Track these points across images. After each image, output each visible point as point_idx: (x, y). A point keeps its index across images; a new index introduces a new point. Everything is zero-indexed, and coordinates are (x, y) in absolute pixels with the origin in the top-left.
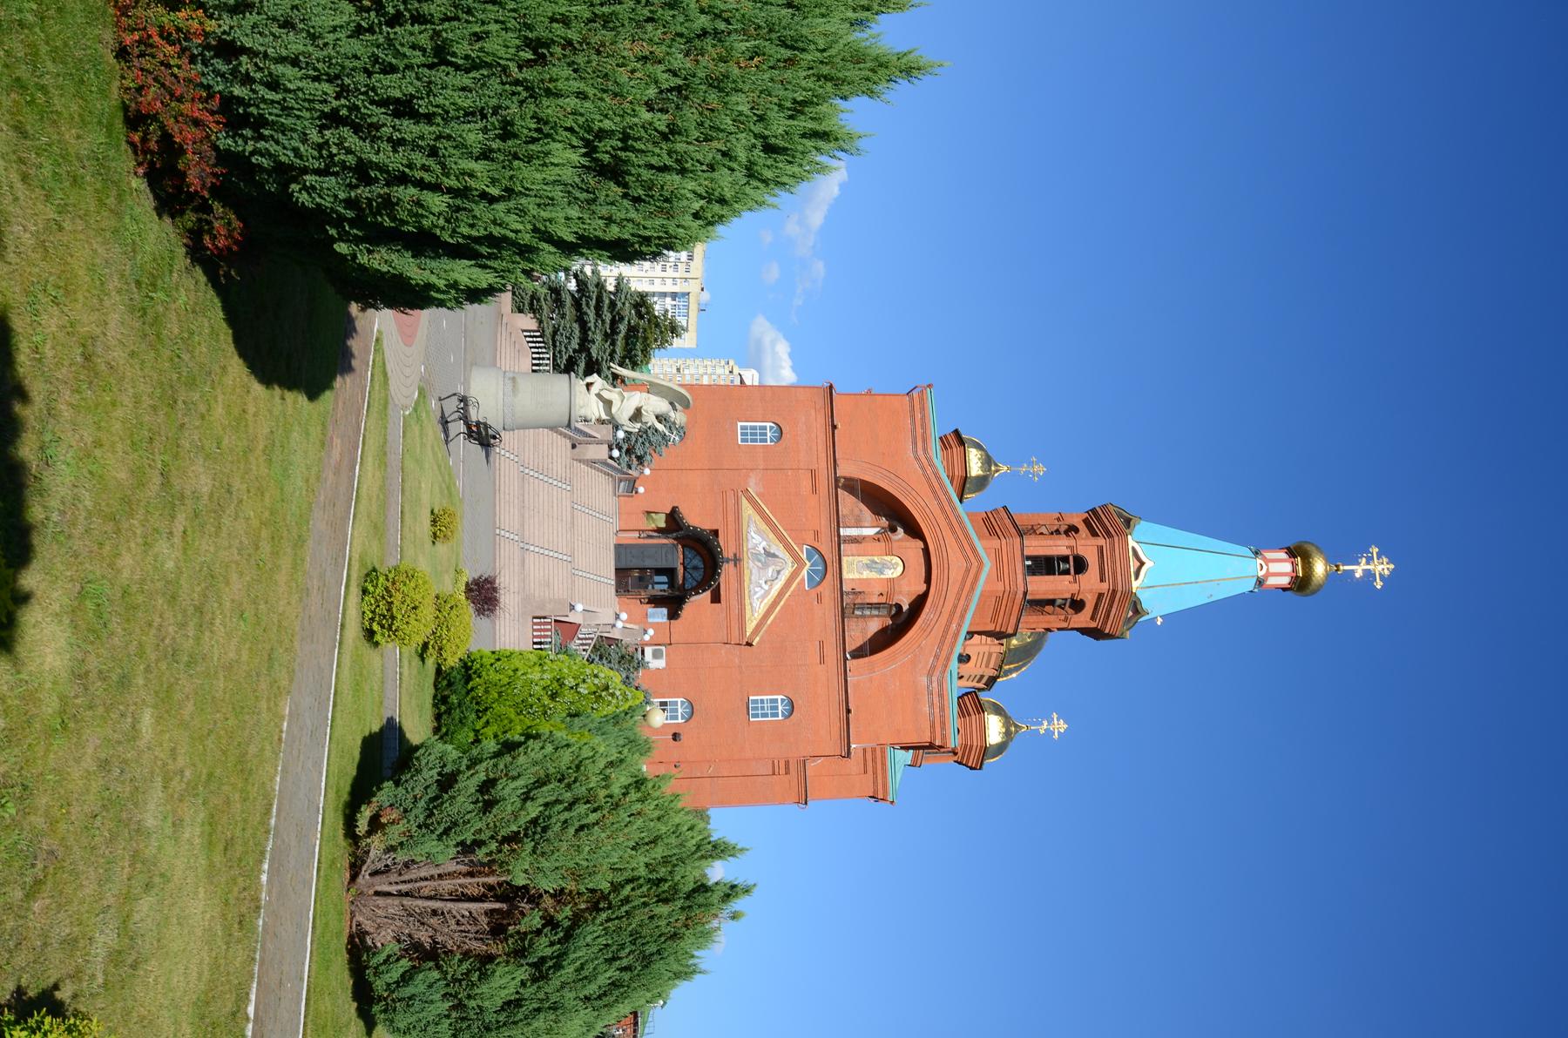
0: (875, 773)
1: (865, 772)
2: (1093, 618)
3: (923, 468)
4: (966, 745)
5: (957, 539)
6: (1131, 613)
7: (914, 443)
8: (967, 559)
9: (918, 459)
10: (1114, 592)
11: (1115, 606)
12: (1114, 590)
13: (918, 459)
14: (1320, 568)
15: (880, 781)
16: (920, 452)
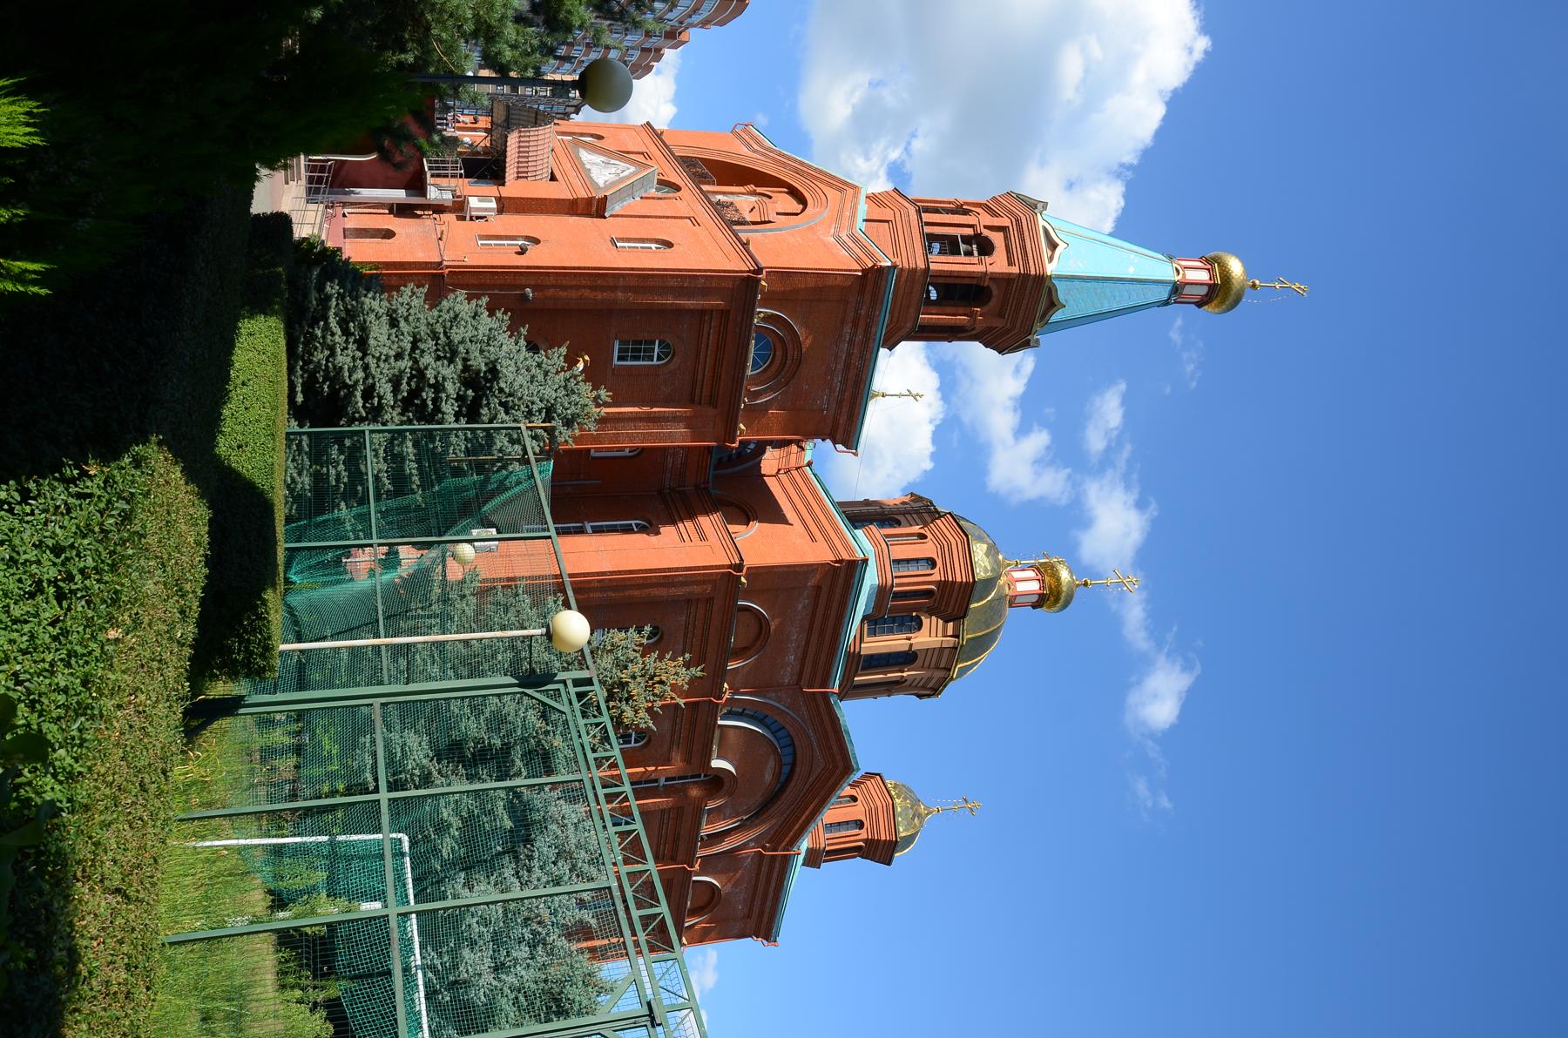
0: (828, 539)
1: (813, 539)
2: (1010, 263)
3: (763, 155)
4: (942, 548)
5: (822, 181)
6: (1050, 253)
7: (748, 145)
8: (840, 190)
9: (755, 151)
10: (1018, 221)
11: (1026, 234)
12: (1017, 220)
13: (755, 151)
14: (1236, 267)
15: (836, 541)
16: (756, 147)
